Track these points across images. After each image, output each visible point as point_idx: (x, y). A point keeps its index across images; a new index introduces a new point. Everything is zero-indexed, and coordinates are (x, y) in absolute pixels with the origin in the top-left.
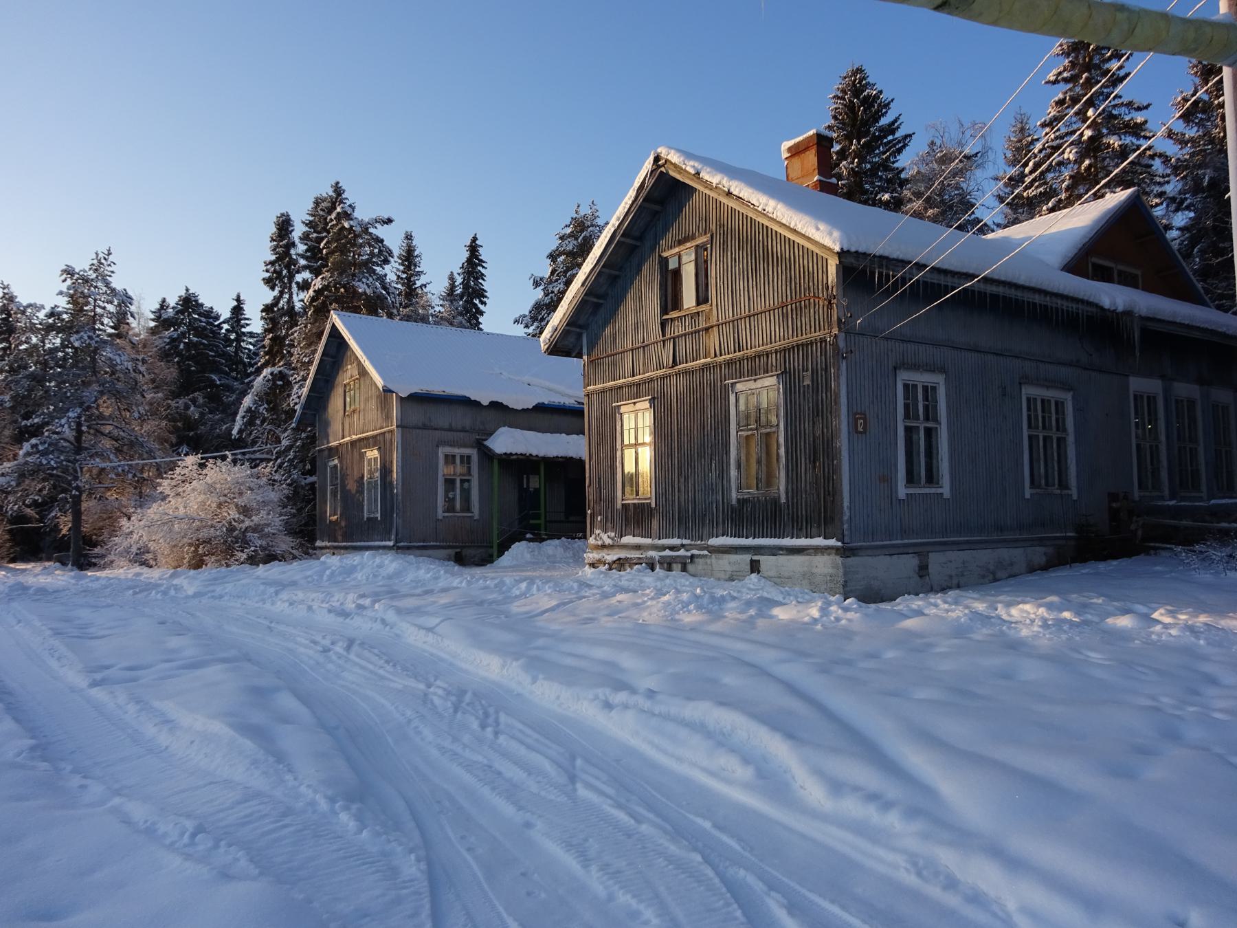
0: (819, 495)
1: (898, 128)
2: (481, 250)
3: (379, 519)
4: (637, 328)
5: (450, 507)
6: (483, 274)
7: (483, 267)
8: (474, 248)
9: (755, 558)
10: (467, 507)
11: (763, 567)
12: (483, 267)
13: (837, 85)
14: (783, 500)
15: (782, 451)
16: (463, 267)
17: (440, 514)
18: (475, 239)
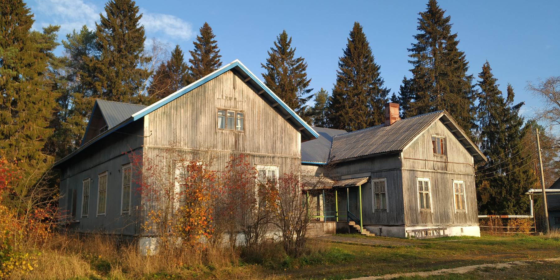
9: (462, 227)
11: (464, 230)
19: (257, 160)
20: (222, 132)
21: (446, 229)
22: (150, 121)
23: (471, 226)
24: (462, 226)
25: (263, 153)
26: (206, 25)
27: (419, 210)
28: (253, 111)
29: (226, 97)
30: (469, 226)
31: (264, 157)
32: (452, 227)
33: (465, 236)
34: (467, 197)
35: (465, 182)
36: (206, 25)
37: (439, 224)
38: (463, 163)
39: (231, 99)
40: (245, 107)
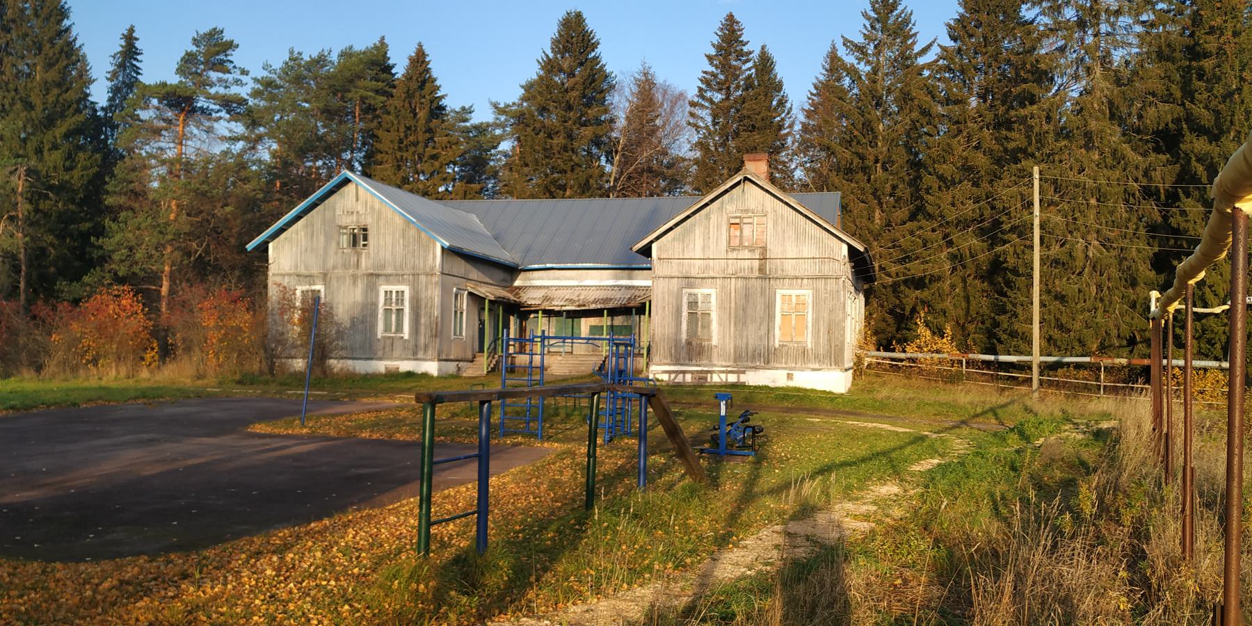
0: (831, 346)
1: (600, 62)
2: (137, 44)
3: (406, 336)
4: (703, 249)
5: (455, 334)
6: (138, 68)
7: (138, 60)
8: (130, 38)
10: (461, 334)
11: (794, 377)
12: (138, 60)
13: (561, 15)
14: (809, 346)
15: (810, 325)
16: (114, 57)
17: (453, 337)
18: (131, 30)
19: (382, 279)
20: (343, 252)
21: (744, 372)
22: (274, 248)
23: (820, 370)
24: (791, 369)
25: (389, 271)
26: (731, 19)
27: (684, 341)
28: (378, 223)
29: (348, 212)
30: (814, 370)
31: (391, 275)
32: (761, 371)
33: (798, 390)
34: (816, 321)
35: (816, 291)
36: (731, 19)
37: (728, 364)
38: (814, 258)
39: (352, 213)
40: (369, 221)
